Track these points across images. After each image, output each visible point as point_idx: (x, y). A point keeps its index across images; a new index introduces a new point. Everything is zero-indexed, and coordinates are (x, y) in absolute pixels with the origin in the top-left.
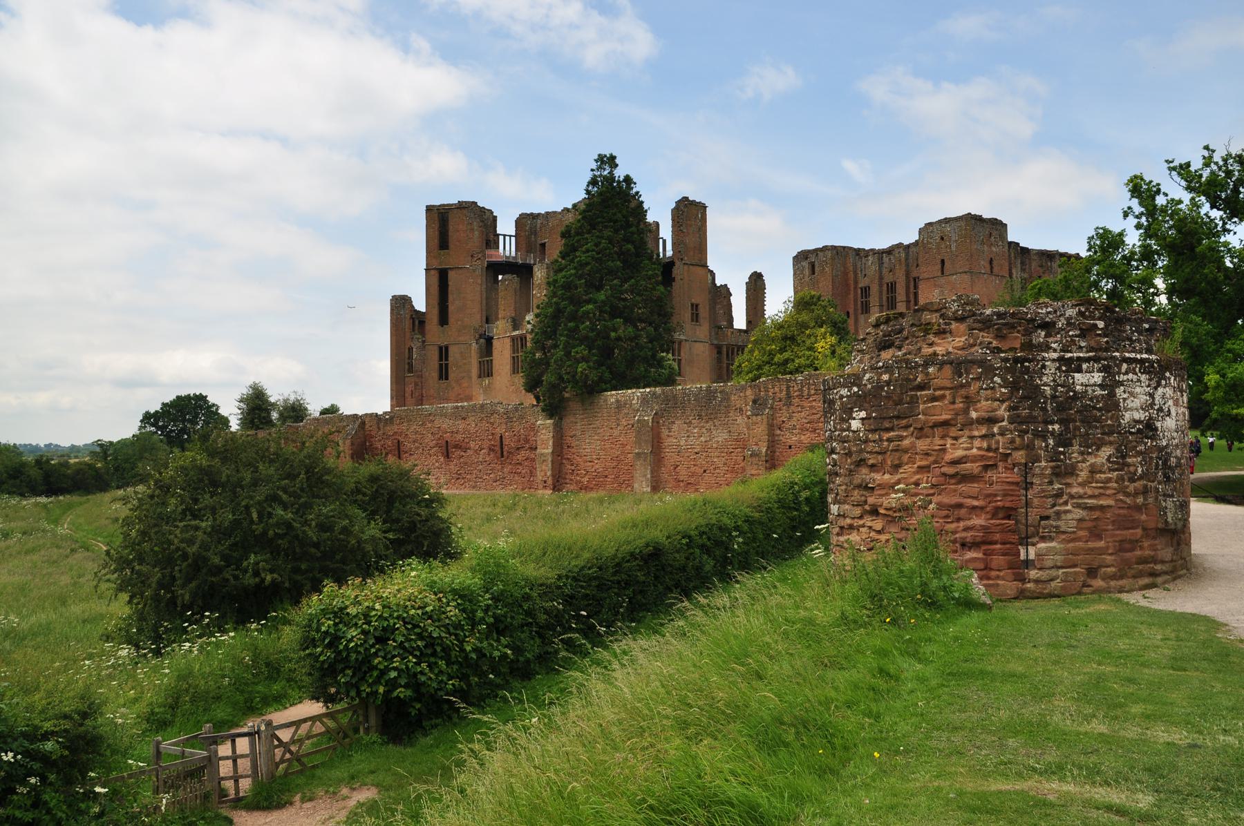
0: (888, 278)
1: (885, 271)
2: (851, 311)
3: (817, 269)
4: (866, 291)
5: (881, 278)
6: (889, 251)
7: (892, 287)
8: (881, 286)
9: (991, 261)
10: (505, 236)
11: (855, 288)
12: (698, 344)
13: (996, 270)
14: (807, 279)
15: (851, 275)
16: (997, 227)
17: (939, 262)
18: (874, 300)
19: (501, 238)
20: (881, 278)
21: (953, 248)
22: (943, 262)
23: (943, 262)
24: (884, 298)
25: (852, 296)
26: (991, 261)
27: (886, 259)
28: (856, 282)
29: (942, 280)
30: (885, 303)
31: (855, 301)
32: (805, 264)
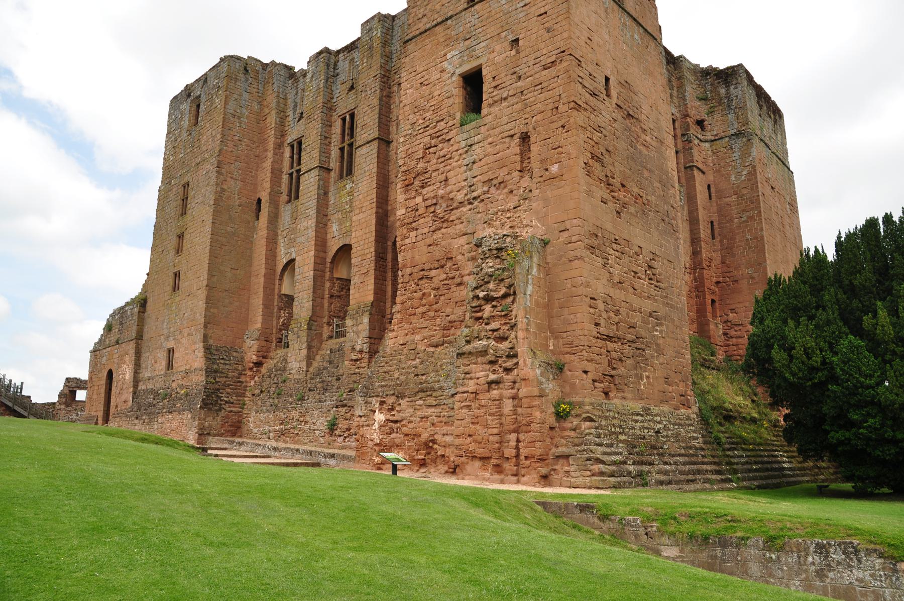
0: (343, 106)
1: (340, 89)
2: (265, 197)
4: (298, 147)
5: (329, 107)
7: (350, 124)
8: (328, 124)
11: (279, 146)
14: (184, 135)
15: (272, 119)
18: (311, 157)
24: (335, 153)
25: (268, 164)
27: (343, 65)
28: (282, 134)
30: (334, 164)
31: (276, 174)
32: (185, 106)
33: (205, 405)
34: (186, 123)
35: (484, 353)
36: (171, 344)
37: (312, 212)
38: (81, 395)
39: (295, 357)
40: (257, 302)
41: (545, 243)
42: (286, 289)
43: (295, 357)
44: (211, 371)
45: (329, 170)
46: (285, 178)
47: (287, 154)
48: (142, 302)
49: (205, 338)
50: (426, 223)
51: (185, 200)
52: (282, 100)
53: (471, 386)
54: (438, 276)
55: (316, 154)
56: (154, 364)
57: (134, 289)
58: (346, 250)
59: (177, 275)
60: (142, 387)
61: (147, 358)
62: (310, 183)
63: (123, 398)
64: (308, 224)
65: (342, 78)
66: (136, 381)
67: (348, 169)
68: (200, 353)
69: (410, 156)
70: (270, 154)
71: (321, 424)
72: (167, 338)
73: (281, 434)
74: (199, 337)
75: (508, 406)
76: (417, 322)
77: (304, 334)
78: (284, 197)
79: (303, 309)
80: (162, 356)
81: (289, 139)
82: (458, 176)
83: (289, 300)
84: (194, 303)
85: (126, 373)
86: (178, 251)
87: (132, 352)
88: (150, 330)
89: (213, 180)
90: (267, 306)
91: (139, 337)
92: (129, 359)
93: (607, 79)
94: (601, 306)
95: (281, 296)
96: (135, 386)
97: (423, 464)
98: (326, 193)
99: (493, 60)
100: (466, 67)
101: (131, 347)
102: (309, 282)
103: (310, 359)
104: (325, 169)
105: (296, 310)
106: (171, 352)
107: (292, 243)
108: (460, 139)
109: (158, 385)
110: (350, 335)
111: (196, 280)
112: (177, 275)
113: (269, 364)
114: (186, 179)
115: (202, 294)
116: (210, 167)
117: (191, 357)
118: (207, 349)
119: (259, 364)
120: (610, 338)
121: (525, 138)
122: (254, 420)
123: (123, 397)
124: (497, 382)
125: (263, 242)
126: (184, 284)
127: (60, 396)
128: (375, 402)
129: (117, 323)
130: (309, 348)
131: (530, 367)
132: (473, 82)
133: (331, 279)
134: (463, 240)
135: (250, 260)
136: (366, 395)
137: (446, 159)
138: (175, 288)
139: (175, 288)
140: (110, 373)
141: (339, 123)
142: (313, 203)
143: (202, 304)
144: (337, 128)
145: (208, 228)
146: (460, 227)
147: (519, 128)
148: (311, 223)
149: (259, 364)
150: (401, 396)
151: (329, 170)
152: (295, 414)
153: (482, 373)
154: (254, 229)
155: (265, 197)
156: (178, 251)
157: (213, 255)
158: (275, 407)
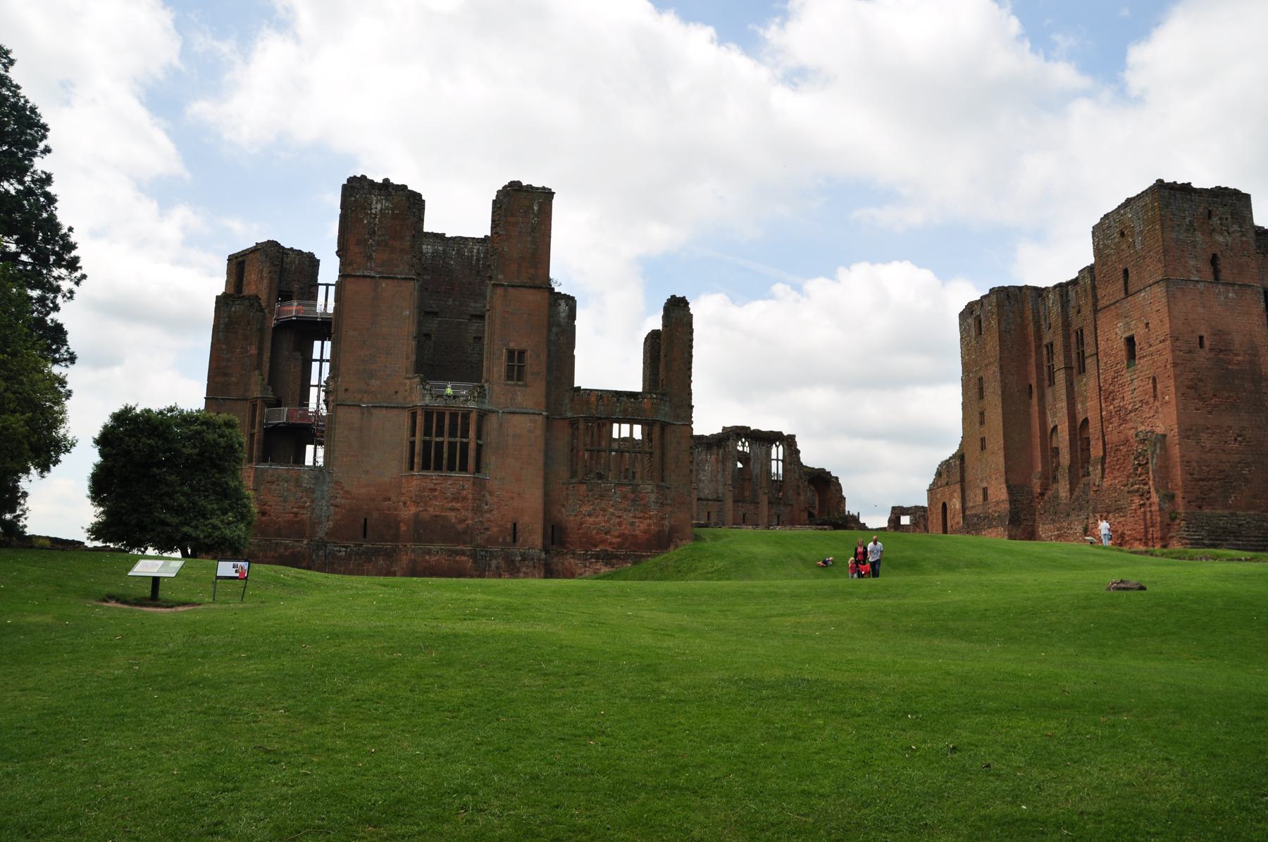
1: (1072, 312)
2: (1034, 382)
3: (983, 325)
5: (1066, 324)
6: (1074, 282)
9: (1214, 260)
10: (327, 285)
11: (1039, 347)
12: (516, 417)
13: (1226, 274)
14: (974, 342)
15: (1031, 329)
16: (1232, 203)
17: (1120, 274)
18: (1059, 362)
19: (322, 290)
20: (1066, 324)
21: (1138, 247)
22: (1126, 272)
23: (1126, 272)
24: (1074, 356)
26: (1214, 260)
27: (1072, 294)
28: (1039, 338)
29: (1126, 305)
30: (1074, 364)
31: (1039, 367)
32: (971, 321)
33: (1011, 522)
34: (973, 333)
35: (1137, 491)
36: (985, 485)
37: (1064, 397)
38: (905, 520)
39: (1063, 489)
40: (1038, 454)
41: (1164, 436)
42: (1054, 445)
43: (1063, 489)
44: (1012, 501)
45: (1071, 368)
46: (1046, 369)
47: (1045, 352)
48: (960, 456)
49: (1007, 481)
50: (1115, 420)
51: (981, 390)
52: (1036, 313)
53: (1134, 507)
54: (1124, 449)
55: (1062, 358)
56: (975, 498)
57: (953, 449)
58: (1086, 421)
59: (983, 440)
60: (968, 513)
61: (970, 494)
62: (1060, 377)
63: (957, 520)
64: (1062, 405)
65: (1072, 303)
66: (964, 509)
67: (1082, 370)
68: (1004, 490)
69: (1105, 381)
70: (1033, 354)
71: (1080, 529)
72: (982, 481)
73: (1058, 537)
74: (1003, 480)
75: (1149, 515)
76: (1117, 474)
77: (1066, 475)
78: (1047, 383)
79: (1065, 458)
80: (979, 492)
81: (1045, 342)
82: (1128, 396)
83: (1056, 451)
84: (997, 459)
85: (956, 504)
86: (982, 423)
87: (959, 490)
88: (969, 475)
89: (998, 378)
90: (1044, 456)
91: (962, 480)
92: (957, 494)
93: (1201, 338)
94: (1194, 464)
95: (1052, 449)
96: (964, 512)
97: (1120, 545)
98: (1072, 384)
99: (1139, 333)
100: (1127, 335)
101: (958, 487)
102: (1067, 443)
103: (1072, 491)
104: (1068, 368)
105: (1061, 460)
106: (985, 490)
107: (1054, 415)
108: (1127, 376)
109: (979, 511)
110: (1092, 476)
111: (996, 442)
112: (983, 440)
113: (1050, 493)
114: (981, 374)
115: (1001, 453)
116: (995, 368)
117: (999, 493)
118: (1008, 487)
119: (1042, 494)
120: (1202, 480)
121: (1154, 379)
122: (1042, 530)
123: (955, 519)
124: (1144, 505)
125: (1037, 414)
126: (989, 446)
127: (889, 521)
128: (1098, 516)
129: (944, 470)
130: (1071, 483)
131: (1155, 498)
132: (1130, 341)
133: (1081, 439)
134: (1132, 431)
135: (1029, 427)
136: (1094, 513)
137: (1122, 385)
138: (983, 448)
139: (983, 448)
140: (944, 505)
141: (1074, 336)
142: (1064, 391)
143: (1002, 460)
144: (1073, 339)
145: (1000, 410)
146: (1131, 425)
147: (1150, 373)
148: (1064, 404)
149: (1042, 494)
150: (1109, 513)
151: (1071, 368)
152: (1065, 524)
153: (1137, 501)
154: (1029, 406)
155: (1034, 382)
156: (982, 423)
157: (1005, 427)
158: (1053, 521)
